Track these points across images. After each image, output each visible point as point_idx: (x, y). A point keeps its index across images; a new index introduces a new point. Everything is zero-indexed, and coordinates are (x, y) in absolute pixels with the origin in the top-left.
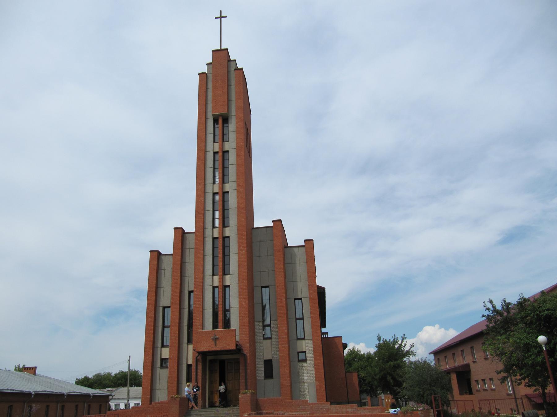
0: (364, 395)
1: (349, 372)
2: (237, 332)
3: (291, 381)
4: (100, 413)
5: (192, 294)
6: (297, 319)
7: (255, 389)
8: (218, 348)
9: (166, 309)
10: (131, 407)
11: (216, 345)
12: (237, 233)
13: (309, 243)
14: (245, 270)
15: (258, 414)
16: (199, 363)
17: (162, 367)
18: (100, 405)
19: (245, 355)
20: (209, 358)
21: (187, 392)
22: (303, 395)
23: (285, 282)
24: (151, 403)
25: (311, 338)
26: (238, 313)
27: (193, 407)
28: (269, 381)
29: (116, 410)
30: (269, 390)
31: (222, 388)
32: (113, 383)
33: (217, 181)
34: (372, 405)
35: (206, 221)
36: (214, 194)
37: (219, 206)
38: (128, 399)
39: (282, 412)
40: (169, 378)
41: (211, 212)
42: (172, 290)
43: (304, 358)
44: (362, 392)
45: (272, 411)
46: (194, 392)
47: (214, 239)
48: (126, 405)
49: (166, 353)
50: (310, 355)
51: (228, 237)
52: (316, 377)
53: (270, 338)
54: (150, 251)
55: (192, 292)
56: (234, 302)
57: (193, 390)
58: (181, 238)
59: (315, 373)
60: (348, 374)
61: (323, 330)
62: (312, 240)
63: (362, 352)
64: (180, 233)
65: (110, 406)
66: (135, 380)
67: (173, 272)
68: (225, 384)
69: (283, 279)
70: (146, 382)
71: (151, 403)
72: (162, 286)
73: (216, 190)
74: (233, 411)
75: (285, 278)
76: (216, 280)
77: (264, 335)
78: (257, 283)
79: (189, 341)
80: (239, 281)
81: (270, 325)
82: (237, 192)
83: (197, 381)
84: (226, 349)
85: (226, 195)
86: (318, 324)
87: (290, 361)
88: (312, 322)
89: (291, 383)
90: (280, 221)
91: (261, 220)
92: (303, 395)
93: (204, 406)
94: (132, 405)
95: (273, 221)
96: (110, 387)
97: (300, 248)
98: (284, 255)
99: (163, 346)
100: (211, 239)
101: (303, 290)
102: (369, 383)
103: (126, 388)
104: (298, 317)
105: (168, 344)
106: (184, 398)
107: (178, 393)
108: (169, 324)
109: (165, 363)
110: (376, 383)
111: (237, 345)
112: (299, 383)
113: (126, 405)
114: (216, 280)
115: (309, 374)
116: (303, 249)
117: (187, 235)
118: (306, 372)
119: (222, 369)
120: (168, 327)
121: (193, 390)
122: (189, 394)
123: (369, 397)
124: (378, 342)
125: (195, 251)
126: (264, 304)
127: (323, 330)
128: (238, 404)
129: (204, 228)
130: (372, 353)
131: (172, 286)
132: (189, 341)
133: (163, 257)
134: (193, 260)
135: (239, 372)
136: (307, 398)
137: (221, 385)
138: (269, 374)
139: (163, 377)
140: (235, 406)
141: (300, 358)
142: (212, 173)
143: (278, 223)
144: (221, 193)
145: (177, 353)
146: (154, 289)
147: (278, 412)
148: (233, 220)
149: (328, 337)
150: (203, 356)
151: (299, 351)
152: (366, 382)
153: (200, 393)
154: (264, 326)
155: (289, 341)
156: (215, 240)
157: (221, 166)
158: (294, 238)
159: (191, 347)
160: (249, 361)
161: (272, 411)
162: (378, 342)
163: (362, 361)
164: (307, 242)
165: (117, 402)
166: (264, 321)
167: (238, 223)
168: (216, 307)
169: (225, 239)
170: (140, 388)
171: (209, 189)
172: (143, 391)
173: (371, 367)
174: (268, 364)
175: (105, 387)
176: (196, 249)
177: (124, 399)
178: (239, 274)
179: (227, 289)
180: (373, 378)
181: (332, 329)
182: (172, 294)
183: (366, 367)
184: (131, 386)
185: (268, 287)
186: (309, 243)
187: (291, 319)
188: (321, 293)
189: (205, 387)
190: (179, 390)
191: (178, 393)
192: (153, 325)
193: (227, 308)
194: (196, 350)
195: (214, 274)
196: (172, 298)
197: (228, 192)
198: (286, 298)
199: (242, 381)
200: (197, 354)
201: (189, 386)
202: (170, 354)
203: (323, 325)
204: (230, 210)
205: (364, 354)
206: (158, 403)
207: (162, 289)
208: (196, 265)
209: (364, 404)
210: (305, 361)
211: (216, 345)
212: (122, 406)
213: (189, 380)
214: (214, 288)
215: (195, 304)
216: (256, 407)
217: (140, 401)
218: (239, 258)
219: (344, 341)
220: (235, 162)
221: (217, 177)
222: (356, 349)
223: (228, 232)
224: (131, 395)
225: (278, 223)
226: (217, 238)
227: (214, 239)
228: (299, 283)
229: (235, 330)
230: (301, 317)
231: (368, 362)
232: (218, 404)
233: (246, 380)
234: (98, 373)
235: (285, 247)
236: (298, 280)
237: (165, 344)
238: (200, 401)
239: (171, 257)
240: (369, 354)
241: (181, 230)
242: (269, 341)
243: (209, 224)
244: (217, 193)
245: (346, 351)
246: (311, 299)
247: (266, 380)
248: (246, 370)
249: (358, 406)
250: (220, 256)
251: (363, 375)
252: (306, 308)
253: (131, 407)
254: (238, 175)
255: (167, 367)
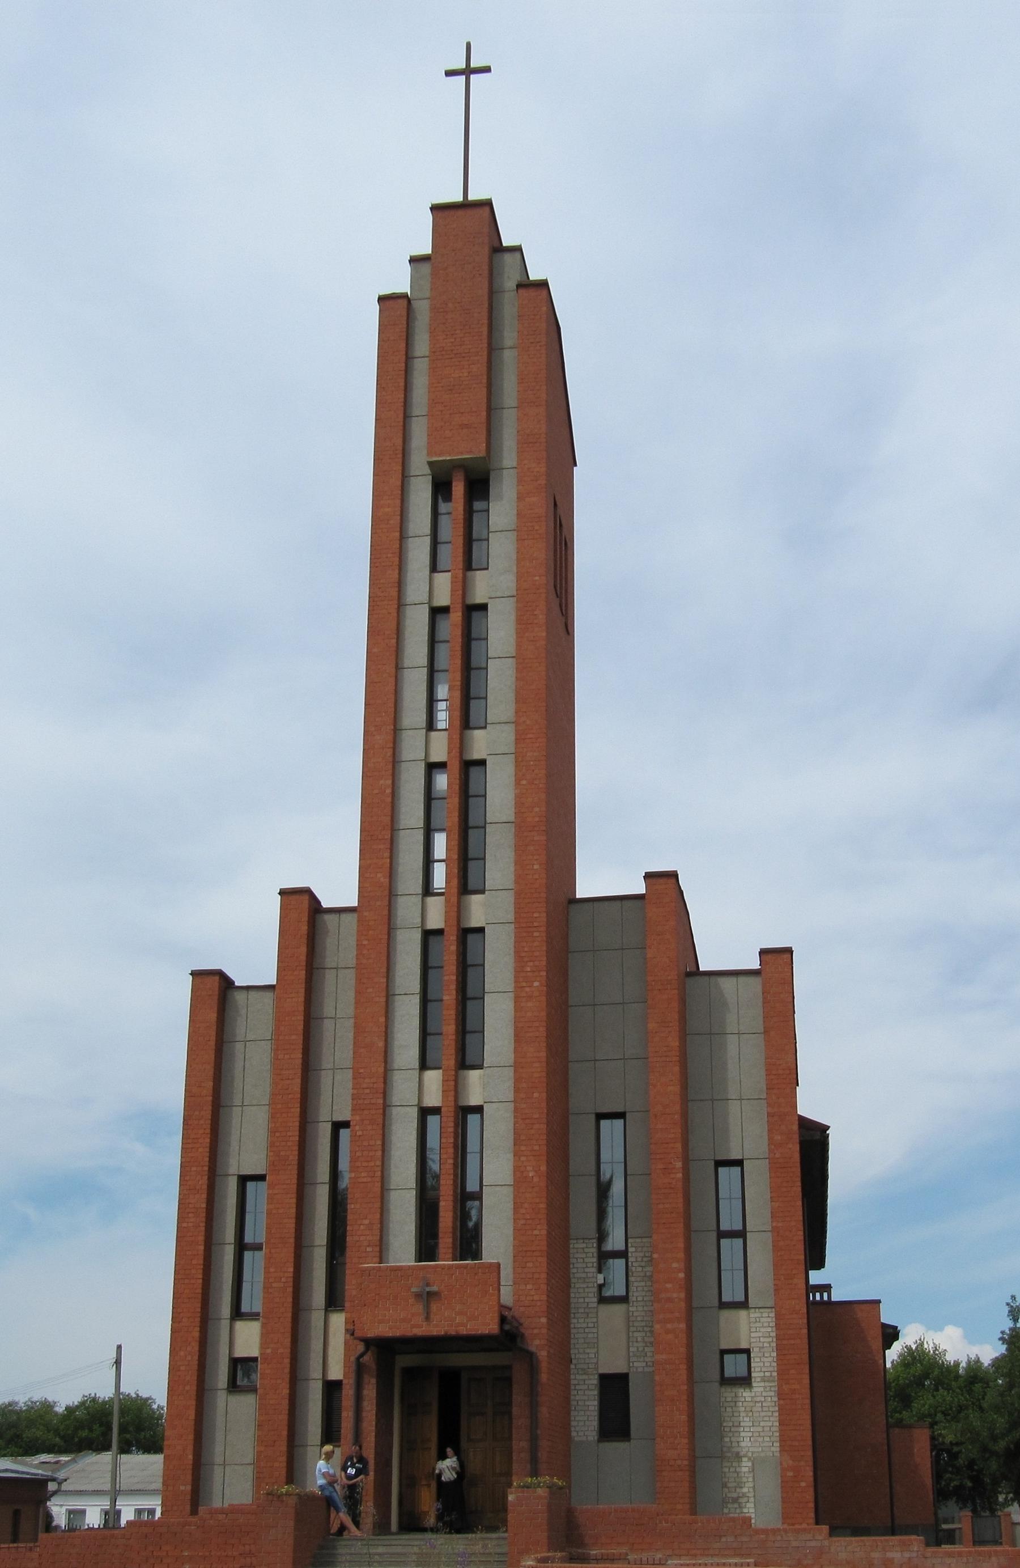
0: (951, 1508)
1: (900, 1424)
2: (507, 1275)
3: (692, 1449)
4: (15, 1539)
5: (344, 1134)
6: (721, 1235)
7: (565, 1471)
8: (436, 1328)
9: (250, 1186)
10: (123, 1523)
11: (427, 1318)
12: (511, 917)
13: (778, 961)
14: (538, 1053)
15: (572, 1559)
16: (366, 1378)
17: (233, 1387)
18: (17, 1513)
19: (531, 1355)
20: (403, 1361)
21: (325, 1475)
22: (735, 1500)
23: (685, 1099)
24: (194, 1511)
25: (771, 1303)
26: (510, 1205)
27: (342, 1529)
28: (615, 1449)
29: (71, 1529)
30: (614, 1479)
31: (447, 1467)
32: (62, 1438)
33: (442, 718)
34: (978, 1542)
35: (401, 869)
36: (432, 768)
37: (447, 813)
38: (115, 1494)
39: (659, 1556)
40: (260, 1426)
41: (420, 836)
42: (273, 1117)
43: (742, 1372)
44: (942, 1495)
45: (623, 1550)
46: (350, 1477)
47: (428, 935)
48: (106, 1513)
49: (247, 1339)
50: (764, 1364)
51: (481, 930)
52: (782, 1440)
53: (624, 1299)
54: (193, 973)
55: (346, 1124)
56: (497, 1167)
57: (344, 1469)
58: (304, 928)
59: (781, 1423)
60: (897, 1430)
61: (816, 1277)
62: (789, 951)
63: (950, 1358)
64: (302, 910)
65: (49, 1517)
66: (139, 1429)
67: (276, 1050)
68: (457, 1453)
69: (675, 1089)
70: (178, 1438)
71: (194, 1511)
72: (237, 1101)
73: (439, 754)
74: (485, 1546)
75: (684, 1086)
76: (433, 1087)
77: (601, 1287)
78: (582, 1100)
79: (334, 1301)
80: (517, 1090)
81: (623, 1254)
82: (517, 762)
83: (358, 1439)
84: (463, 1331)
85: (474, 771)
86: (799, 1253)
87: (691, 1380)
88: (776, 1248)
89: (693, 1458)
90: (673, 876)
91: (603, 872)
92: (735, 1500)
93: (382, 1527)
94: (127, 1515)
95: (648, 876)
96: (49, 1450)
97: (742, 979)
98: (683, 1001)
99: (237, 1313)
100: (417, 936)
101: (747, 1133)
102: (971, 1464)
103: (106, 1457)
104: (725, 1226)
105: (258, 1307)
106: (311, 1498)
107: (290, 1479)
108: (261, 1238)
109: (247, 1374)
110: (994, 1465)
111: (503, 1320)
112: (722, 1457)
113: (106, 1513)
114: (433, 1087)
115: (758, 1429)
116: (756, 983)
117: (327, 917)
118: (746, 1422)
119: (448, 1401)
120: (258, 1247)
121: (344, 1469)
122: (331, 1483)
123: (967, 1513)
124: (1011, 1324)
125: (359, 980)
126: (605, 1176)
127: (816, 1277)
128: (505, 1522)
129: (392, 894)
130: (986, 1360)
131: (272, 1103)
132: (334, 1301)
133: (240, 997)
134: (351, 1011)
135: (510, 1413)
136: (749, 1509)
137: (443, 1456)
138: (615, 1423)
139: (238, 1424)
140: (492, 1528)
141: (729, 1373)
142: (423, 687)
143: (664, 884)
144: (455, 766)
145: (287, 1341)
146: (207, 1113)
147: (644, 1556)
148: (499, 866)
149: (830, 1303)
150: (382, 1353)
151: (724, 1346)
152: (961, 1461)
153: (368, 1482)
154: (604, 1257)
155: (690, 1310)
156: (432, 940)
157: (458, 662)
158: (723, 940)
159: (338, 1321)
160: (544, 1377)
161: (623, 1550)
162: (1011, 1324)
163: (949, 1389)
164: (768, 957)
165: (77, 1503)
166: (602, 1236)
167: (519, 878)
168: (430, 1182)
169: (469, 936)
170: (158, 1459)
171: (413, 748)
172: (166, 1469)
173: (981, 1409)
174: (614, 1389)
175: (31, 1449)
176: (361, 971)
177: (98, 1495)
178: (517, 1066)
179: (473, 1119)
180: (985, 1449)
181: (842, 1276)
182: (272, 1132)
183: (961, 1408)
184: (125, 1449)
185: (621, 1115)
186: (778, 961)
187: (699, 1233)
188: (813, 1143)
189: (388, 1463)
190: (293, 1469)
191: (290, 1479)
192: (201, 1238)
193: (472, 1186)
194: (358, 1334)
195: (424, 1065)
196: (271, 1145)
197: (482, 763)
198: (686, 1160)
199: (520, 1444)
200: (361, 1347)
201: (329, 1456)
202: (264, 1345)
203: (816, 1258)
204: (489, 829)
205: (957, 1364)
206: (221, 1511)
207: (236, 1111)
208: (359, 1030)
209: (950, 1538)
210: (746, 1381)
211: (427, 1318)
212: (94, 1518)
213: (330, 1435)
214: (425, 1112)
215: (353, 1169)
216: (568, 1532)
217: (156, 1504)
218: (518, 1008)
219: (887, 1317)
220: (511, 650)
221: (442, 706)
222: (929, 1346)
223: (477, 911)
224: (125, 1481)
225: (664, 884)
226: (440, 932)
227: (428, 935)
228: (734, 1108)
229: (498, 1266)
230: (739, 1227)
231: (970, 1392)
232: (431, 1521)
233: (534, 1441)
234: (7, 1401)
235: (689, 975)
236: (733, 1094)
237: (245, 1308)
238: (368, 1508)
239: (269, 996)
240: (974, 1366)
241: (306, 898)
242: (619, 1309)
243: (410, 879)
244: (442, 766)
245: (893, 1354)
246: (776, 1166)
247: (601, 1445)
248: (533, 1406)
249: (928, 1544)
250: (449, 997)
251: (950, 1438)
252: (756, 1198)
253: (123, 1523)
254: (520, 699)
255: (253, 1390)
